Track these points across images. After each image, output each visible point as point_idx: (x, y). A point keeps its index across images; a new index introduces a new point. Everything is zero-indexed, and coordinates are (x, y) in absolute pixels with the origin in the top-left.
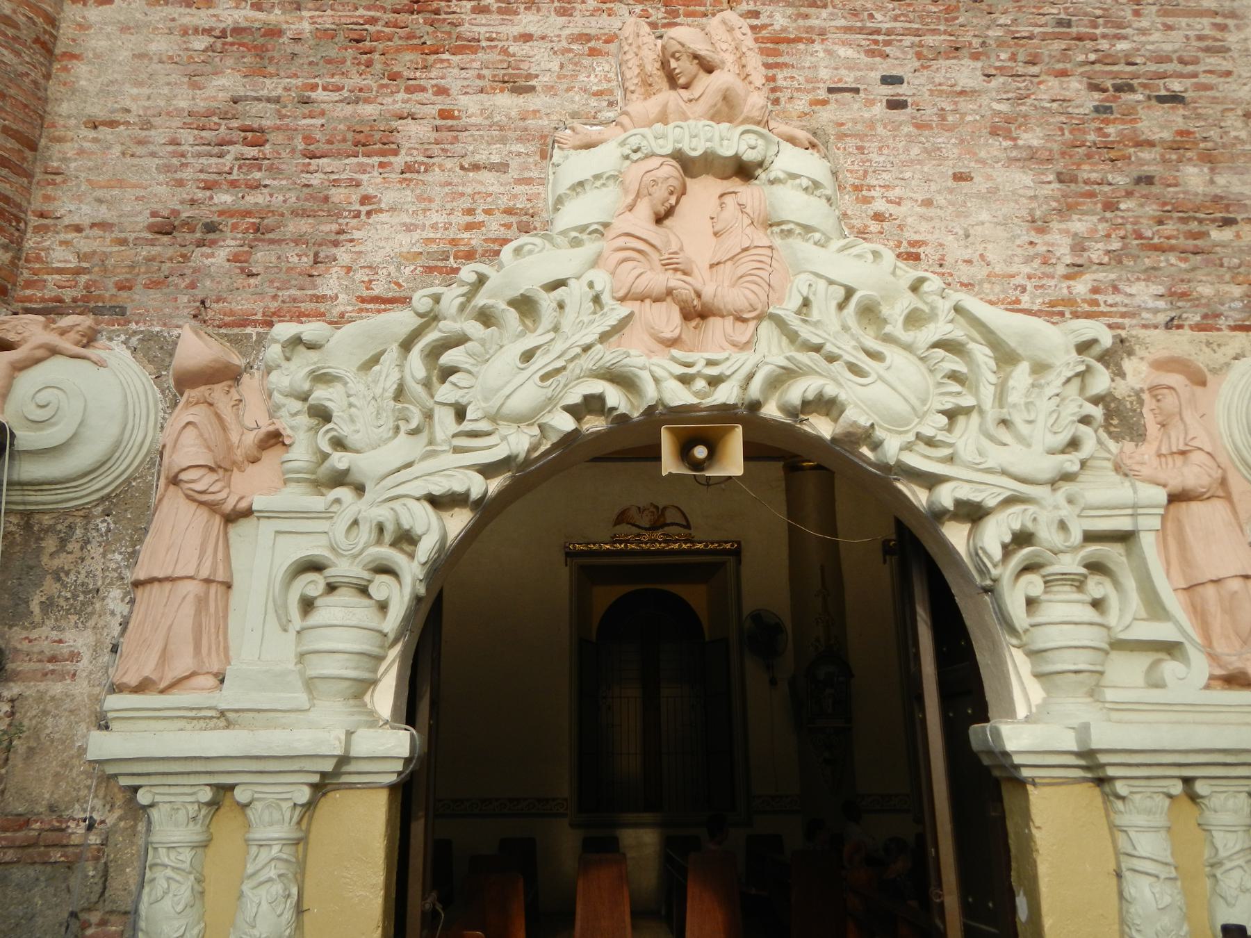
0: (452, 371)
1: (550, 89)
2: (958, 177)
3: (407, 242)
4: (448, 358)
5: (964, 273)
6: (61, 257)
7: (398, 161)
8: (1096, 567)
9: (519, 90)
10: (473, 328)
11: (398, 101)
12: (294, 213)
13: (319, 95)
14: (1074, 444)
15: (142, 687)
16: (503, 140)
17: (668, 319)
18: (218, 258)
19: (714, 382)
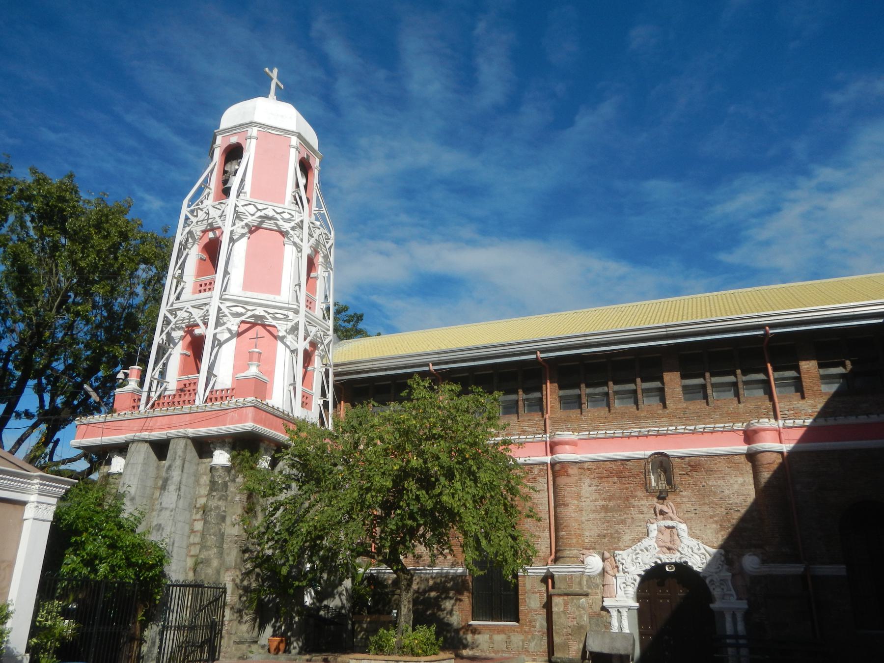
0: (637, 558)
1: (646, 513)
2: (705, 526)
3: (630, 538)
4: (638, 556)
5: (706, 541)
6: (587, 541)
7: (627, 525)
8: (721, 584)
9: (642, 514)
10: (640, 552)
11: (626, 516)
12: (615, 534)
13: (615, 515)
14: (719, 568)
15: (608, 597)
16: (640, 522)
17: (665, 550)
18: (606, 540)
19: (671, 559)
